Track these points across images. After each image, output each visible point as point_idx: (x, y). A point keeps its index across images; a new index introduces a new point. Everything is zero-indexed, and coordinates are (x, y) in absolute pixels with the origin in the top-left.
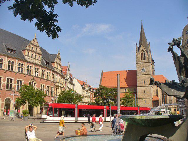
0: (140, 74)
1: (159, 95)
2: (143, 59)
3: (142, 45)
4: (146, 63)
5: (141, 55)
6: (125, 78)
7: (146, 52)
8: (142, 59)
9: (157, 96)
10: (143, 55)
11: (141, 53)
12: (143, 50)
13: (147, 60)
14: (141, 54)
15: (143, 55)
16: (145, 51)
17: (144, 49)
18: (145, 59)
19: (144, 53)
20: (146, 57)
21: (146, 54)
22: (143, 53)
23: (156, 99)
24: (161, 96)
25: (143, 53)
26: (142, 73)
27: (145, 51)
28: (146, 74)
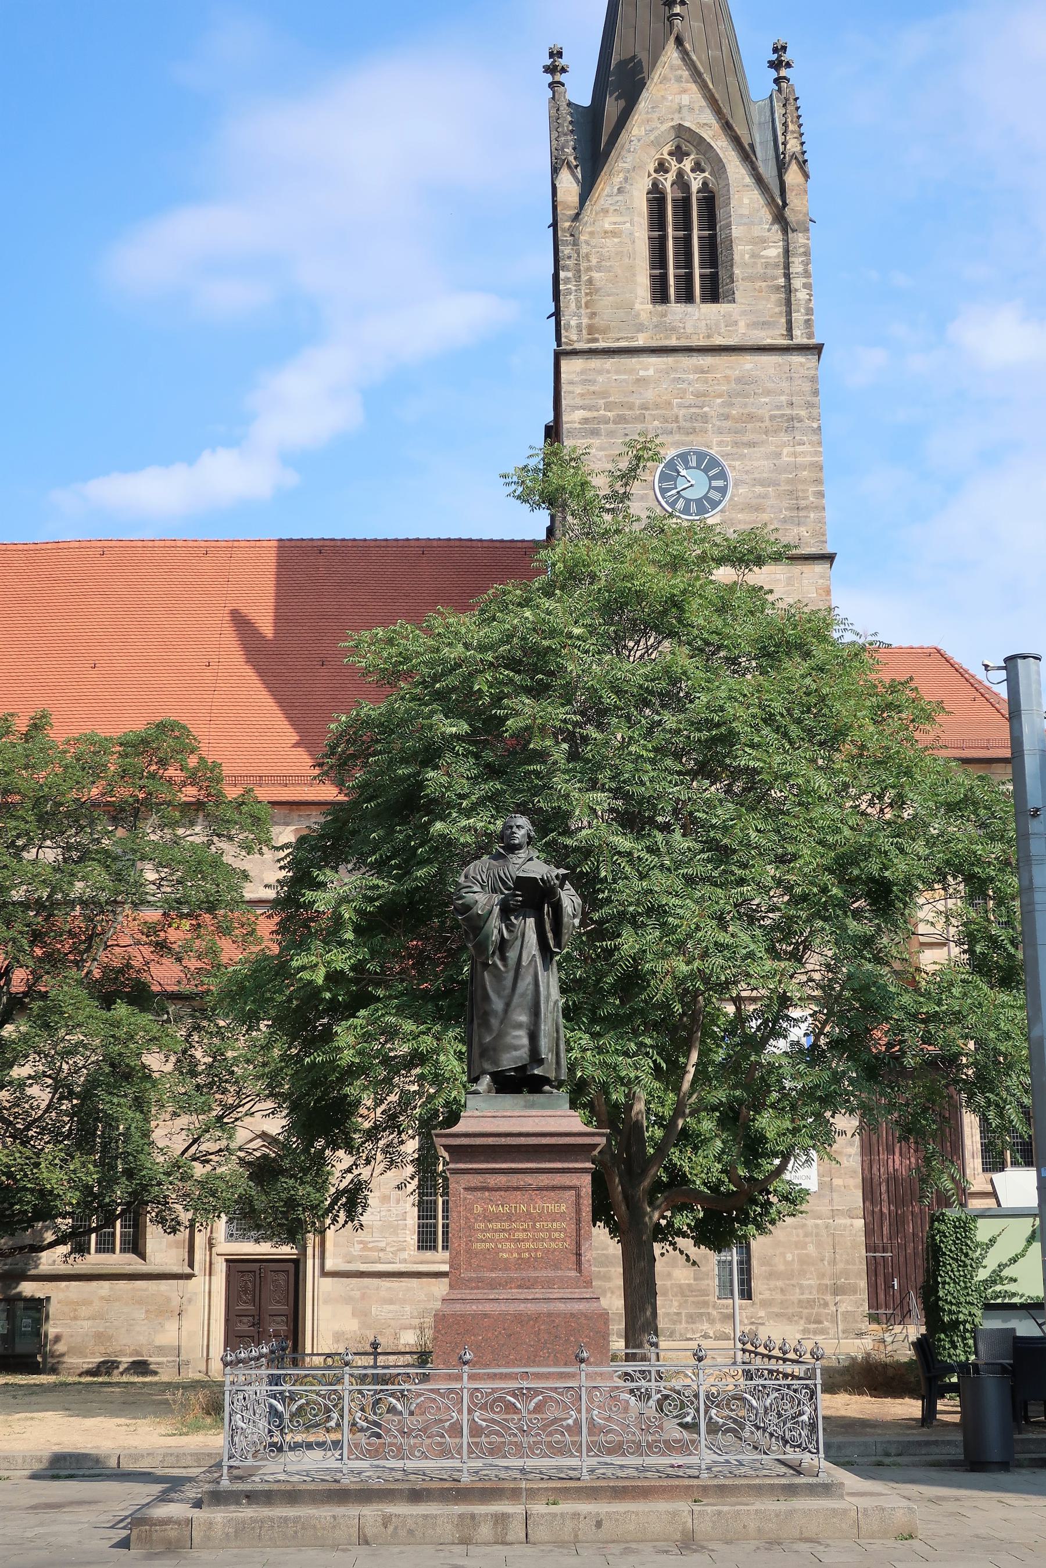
2: (687, 297)
3: (671, 55)
4: (748, 363)
5: (657, 220)
7: (736, 170)
8: (660, 294)
11: (657, 199)
13: (771, 305)
14: (641, 204)
18: (714, 293)
19: (710, 202)
22: (681, 182)
25: (681, 182)
27: (722, 145)
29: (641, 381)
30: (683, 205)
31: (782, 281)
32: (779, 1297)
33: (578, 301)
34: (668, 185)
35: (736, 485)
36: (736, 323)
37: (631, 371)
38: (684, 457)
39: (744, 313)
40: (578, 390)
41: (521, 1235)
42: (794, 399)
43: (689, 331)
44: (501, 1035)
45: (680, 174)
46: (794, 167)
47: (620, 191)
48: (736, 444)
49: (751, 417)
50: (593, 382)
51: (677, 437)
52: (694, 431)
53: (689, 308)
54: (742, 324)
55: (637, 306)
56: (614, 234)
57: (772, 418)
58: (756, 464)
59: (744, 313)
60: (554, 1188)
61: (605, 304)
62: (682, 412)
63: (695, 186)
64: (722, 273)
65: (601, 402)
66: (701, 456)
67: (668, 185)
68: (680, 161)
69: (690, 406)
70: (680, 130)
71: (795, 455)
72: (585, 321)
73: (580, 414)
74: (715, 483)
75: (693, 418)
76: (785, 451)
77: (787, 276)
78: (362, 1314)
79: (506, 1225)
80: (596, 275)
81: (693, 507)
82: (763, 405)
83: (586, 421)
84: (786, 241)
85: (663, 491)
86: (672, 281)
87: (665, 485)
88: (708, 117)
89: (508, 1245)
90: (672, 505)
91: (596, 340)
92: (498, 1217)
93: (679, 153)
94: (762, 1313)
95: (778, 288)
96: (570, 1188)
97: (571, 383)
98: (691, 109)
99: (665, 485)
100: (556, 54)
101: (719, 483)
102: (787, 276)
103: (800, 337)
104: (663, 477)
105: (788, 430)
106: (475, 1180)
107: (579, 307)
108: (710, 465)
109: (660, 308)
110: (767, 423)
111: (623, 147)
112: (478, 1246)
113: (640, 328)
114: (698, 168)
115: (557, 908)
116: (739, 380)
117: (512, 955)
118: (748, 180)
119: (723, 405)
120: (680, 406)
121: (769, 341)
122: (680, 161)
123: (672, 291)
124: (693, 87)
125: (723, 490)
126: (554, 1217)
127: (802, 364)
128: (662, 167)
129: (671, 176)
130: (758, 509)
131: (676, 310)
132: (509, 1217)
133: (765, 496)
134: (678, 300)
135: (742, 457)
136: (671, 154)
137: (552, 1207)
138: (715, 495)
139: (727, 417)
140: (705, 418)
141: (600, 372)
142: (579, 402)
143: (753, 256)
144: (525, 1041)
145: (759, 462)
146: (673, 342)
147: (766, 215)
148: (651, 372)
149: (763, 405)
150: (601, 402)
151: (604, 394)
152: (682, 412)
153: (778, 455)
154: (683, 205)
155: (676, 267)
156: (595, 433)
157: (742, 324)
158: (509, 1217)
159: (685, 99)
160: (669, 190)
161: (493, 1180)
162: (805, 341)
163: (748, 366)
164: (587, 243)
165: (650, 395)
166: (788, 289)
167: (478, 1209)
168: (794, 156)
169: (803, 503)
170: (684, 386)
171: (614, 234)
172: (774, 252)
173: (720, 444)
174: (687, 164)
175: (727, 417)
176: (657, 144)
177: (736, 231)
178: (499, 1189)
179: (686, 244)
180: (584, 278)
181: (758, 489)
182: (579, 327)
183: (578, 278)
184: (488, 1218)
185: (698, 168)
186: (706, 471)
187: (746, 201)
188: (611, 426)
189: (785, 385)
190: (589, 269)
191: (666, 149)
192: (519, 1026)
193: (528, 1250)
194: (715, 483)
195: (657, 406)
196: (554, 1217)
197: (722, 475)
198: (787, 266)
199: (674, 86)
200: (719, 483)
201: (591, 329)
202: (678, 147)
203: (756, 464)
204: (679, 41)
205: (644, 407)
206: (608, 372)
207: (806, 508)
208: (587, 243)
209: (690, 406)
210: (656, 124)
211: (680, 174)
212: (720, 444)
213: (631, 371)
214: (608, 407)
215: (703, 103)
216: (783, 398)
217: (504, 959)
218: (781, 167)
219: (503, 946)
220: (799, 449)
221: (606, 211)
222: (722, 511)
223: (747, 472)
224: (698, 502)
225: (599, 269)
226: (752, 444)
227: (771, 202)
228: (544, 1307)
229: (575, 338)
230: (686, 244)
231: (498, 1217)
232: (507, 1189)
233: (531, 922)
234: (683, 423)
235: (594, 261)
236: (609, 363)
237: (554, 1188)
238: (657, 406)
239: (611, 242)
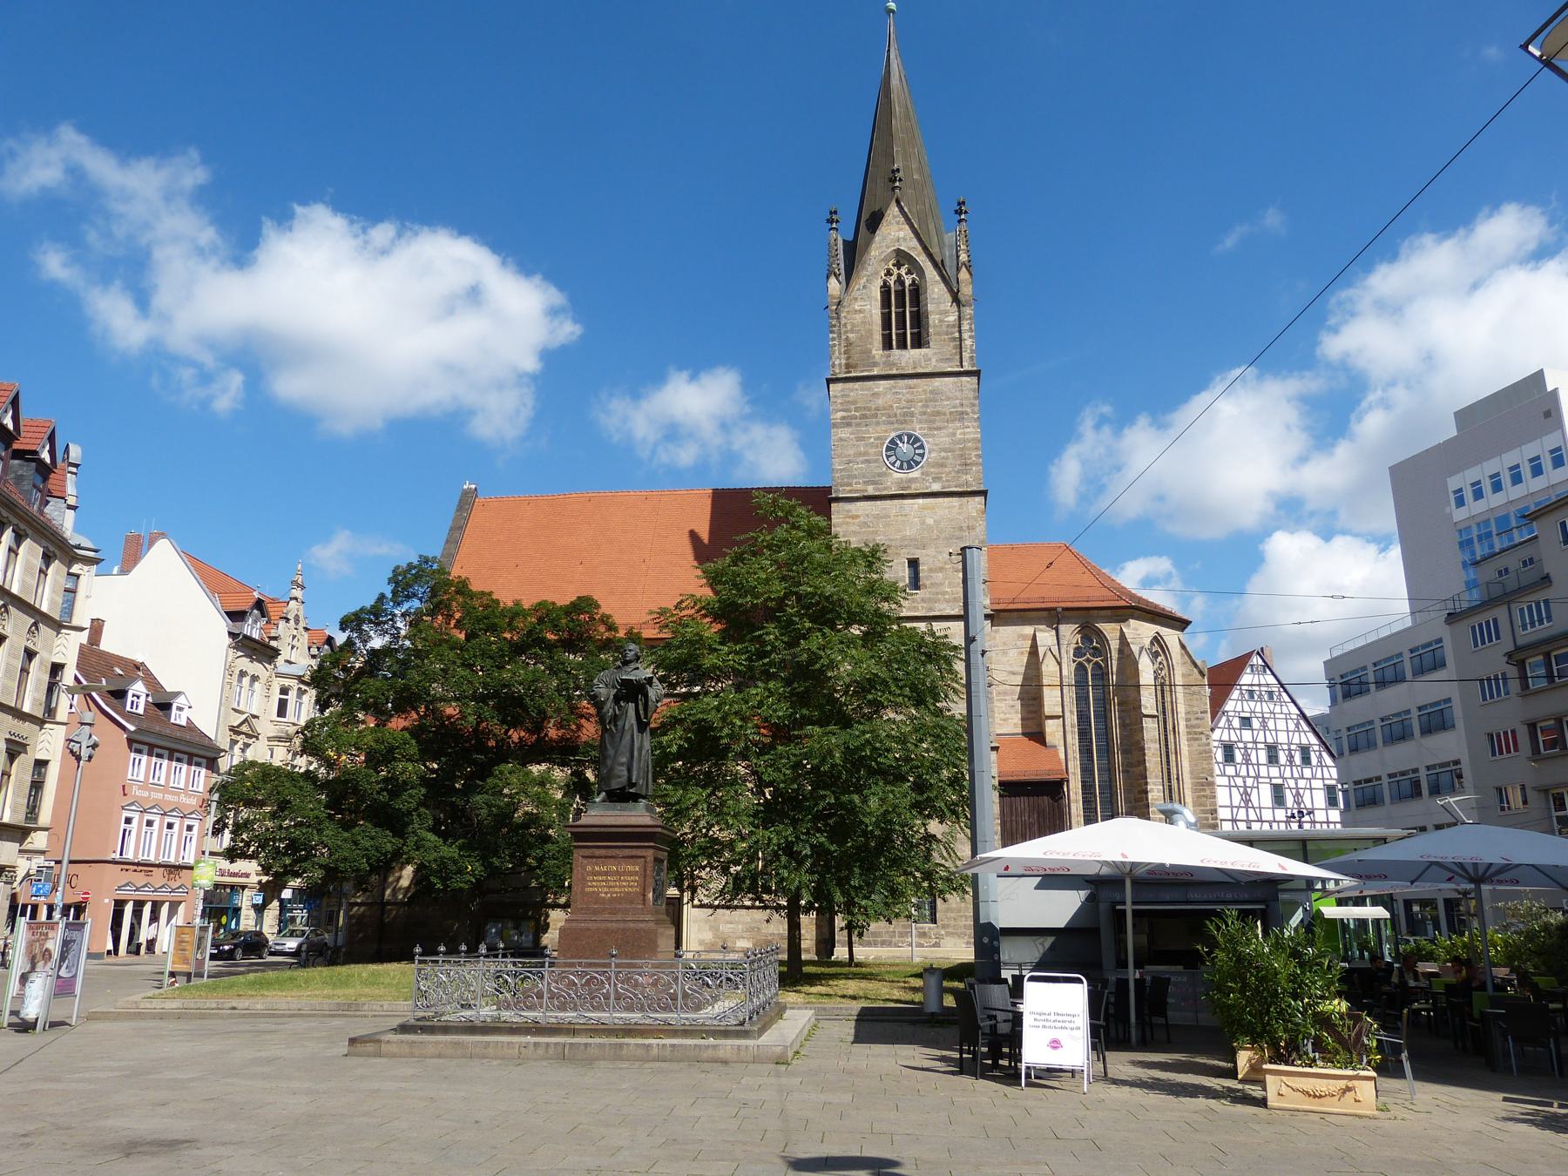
0: (871, 491)
1: (1052, 729)
2: (902, 345)
4: (937, 382)
6: (693, 535)
7: (931, 273)
8: (887, 345)
9: (1036, 735)
10: (901, 304)
12: (902, 258)
13: (950, 348)
14: (877, 294)
15: (901, 304)
16: (922, 260)
17: (911, 246)
18: (919, 342)
19: (917, 292)
20: (933, 319)
21: (936, 291)
22: (900, 281)
23: (1032, 765)
24: (1074, 740)
25: (900, 281)
26: (895, 478)
27: (922, 260)
28: (936, 487)
29: (876, 395)
30: (901, 295)
31: (957, 335)
32: (952, 923)
33: (839, 350)
34: (892, 283)
35: (930, 452)
36: (930, 360)
37: (869, 389)
38: (900, 437)
39: (935, 354)
40: (839, 401)
41: (612, 884)
42: (964, 402)
43: (903, 364)
44: (611, 770)
45: (899, 276)
46: (964, 269)
47: (864, 287)
48: (930, 429)
49: (938, 413)
50: (848, 396)
51: (896, 426)
52: (906, 422)
53: (904, 352)
54: (934, 360)
55: (874, 352)
56: (860, 311)
57: (951, 413)
58: (941, 440)
59: (935, 354)
60: (632, 857)
61: (855, 351)
62: (899, 411)
63: (907, 283)
64: (924, 334)
65: (853, 407)
66: (909, 436)
67: (892, 283)
68: (899, 269)
70: (899, 252)
71: (964, 434)
72: (843, 362)
73: (840, 414)
74: (917, 451)
75: (905, 414)
76: (958, 432)
77: (960, 332)
78: (715, 929)
79: (604, 878)
80: (850, 335)
81: (905, 464)
82: (946, 406)
83: (844, 418)
84: (959, 311)
85: (888, 457)
86: (894, 337)
87: (889, 453)
88: (915, 243)
89: (606, 890)
90: (893, 464)
91: (850, 372)
92: (600, 873)
93: (898, 265)
94: (943, 932)
95: (955, 339)
96: (643, 857)
97: (835, 397)
98: (905, 239)
99: (889, 453)
101: (921, 451)
102: (960, 332)
103: (967, 367)
104: (888, 449)
105: (961, 420)
106: (587, 852)
107: (840, 354)
108: (914, 440)
109: (886, 352)
111: (865, 262)
112: (588, 889)
113: (875, 364)
114: (909, 272)
115: (646, 696)
116: (931, 392)
117: (620, 723)
118: (938, 278)
119: (923, 406)
121: (949, 369)
122: (899, 269)
123: (894, 343)
124: (907, 227)
125: (922, 455)
126: (631, 874)
127: (968, 382)
128: (889, 273)
129: (894, 278)
130: (943, 465)
131: (896, 352)
132: (606, 874)
133: (947, 458)
134: (898, 348)
135: (933, 436)
136: (894, 265)
137: (630, 868)
138: (917, 458)
139: (925, 413)
140: (912, 415)
141: (852, 390)
142: (839, 407)
143: (940, 321)
144: (625, 773)
145: (943, 439)
146: (894, 372)
147: (948, 297)
148: (881, 389)
149: (946, 406)
150: (853, 407)
151: (854, 402)
152: (899, 411)
153: (954, 434)
154: (901, 295)
155: (897, 329)
156: (849, 425)
157: (934, 360)
158: (606, 874)
159: (902, 234)
160: (892, 286)
161: (597, 852)
162: (970, 369)
163: (936, 384)
164: (845, 317)
165: (880, 402)
166: (961, 339)
167: (589, 868)
168: (964, 264)
169: (969, 461)
170: (900, 396)
171: (860, 311)
172: (952, 318)
173: (920, 429)
174: (903, 271)
175: (925, 413)
176: (886, 260)
177: (930, 307)
178: (601, 857)
179: (902, 316)
180: (843, 337)
181: (943, 454)
182: (840, 364)
183: (840, 337)
184: (595, 874)
185: (909, 272)
186: (912, 444)
187: (936, 290)
188: (858, 420)
189: (958, 394)
190: (846, 332)
191: (891, 262)
192: (622, 764)
193: (617, 893)
194: (917, 451)
195: (885, 409)
196: (631, 874)
197: (922, 447)
198: (960, 327)
199: (896, 227)
200: (921, 451)
201: (848, 366)
202: (898, 261)
203: (941, 440)
204: (898, 202)
205: (877, 409)
207: (970, 464)
208: (845, 317)
210: (884, 249)
211: (899, 276)
212: (920, 429)
213: (869, 389)
215: (912, 235)
216: (957, 401)
217: (616, 726)
218: (958, 270)
219: (615, 718)
220: (968, 430)
221: (856, 299)
222: (922, 467)
223: (936, 445)
224: (908, 462)
225: (852, 331)
226: (939, 429)
227: (950, 290)
228: (621, 925)
229: (837, 371)
230: (902, 316)
231: (600, 873)
232: (606, 857)
233: (631, 706)
234: (899, 418)
235: (849, 328)
236: (857, 385)
237: (632, 857)
238: (885, 409)
239: (858, 317)
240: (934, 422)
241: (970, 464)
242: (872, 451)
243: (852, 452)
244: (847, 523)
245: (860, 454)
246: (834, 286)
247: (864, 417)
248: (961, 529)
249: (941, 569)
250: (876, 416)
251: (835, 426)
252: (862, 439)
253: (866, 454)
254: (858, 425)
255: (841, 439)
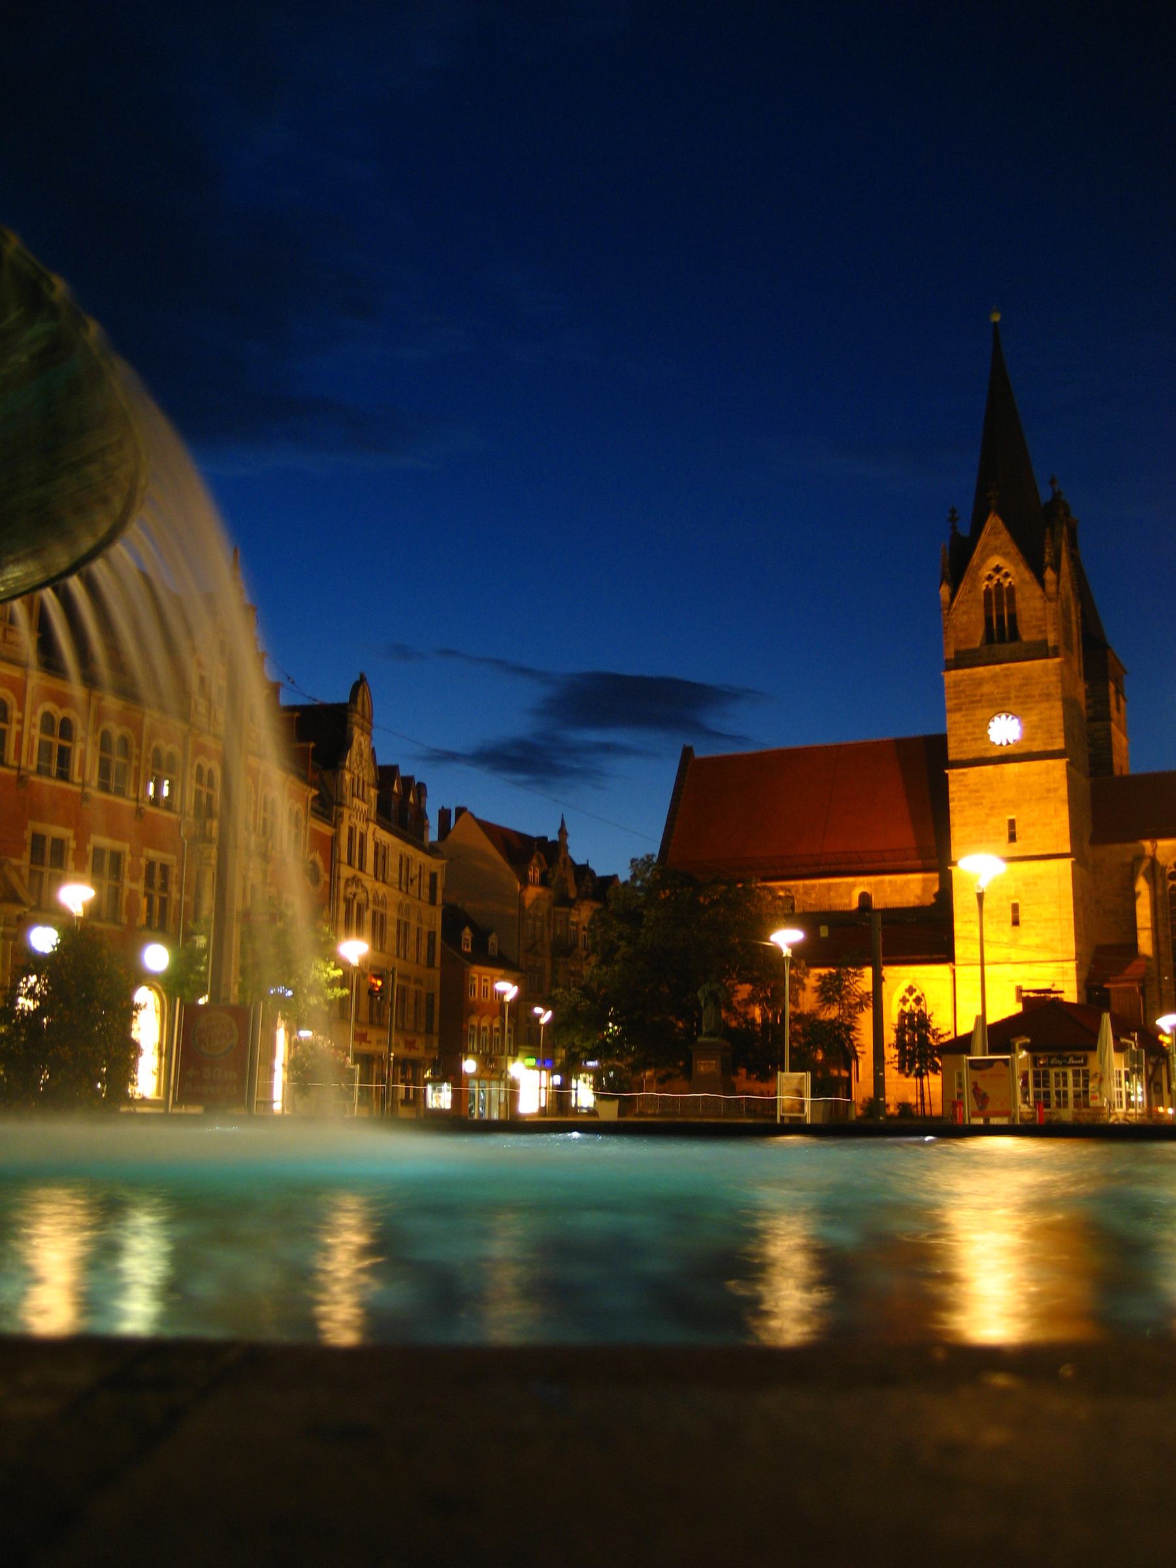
2: (1002, 640)
10: (1000, 604)
15: (1000, 604)
62: (998, 696)
69: (1002, 694)
75: (1003, 699)
83: (956, 704)
100: (953, 511)
110: (1037, 698)
120: (997, 693)
131: (996, 646)
142: (952, 696)
151: (963, 691)
156: (960, 710)
188: (967, 706)
205: (982, 695)
206: (965, 680)
209: (1002, 694)
214: (966, 696)
226: (1030, 709)
234: (999, 701)
240: (1025, 703)
241: (1055, 738)
242: (977, 730)
243: (963, 732)
244: (960, 791)
245: (969, 734)
246: (945, 591)
247: (973, 702)
248: (1049, 791)
249: (1033, 825)
250: (980, 701)
251: (950, 711)
252: (970, 721)
253: (974, 733)
254: (967, 709)
255: (954, 723)
